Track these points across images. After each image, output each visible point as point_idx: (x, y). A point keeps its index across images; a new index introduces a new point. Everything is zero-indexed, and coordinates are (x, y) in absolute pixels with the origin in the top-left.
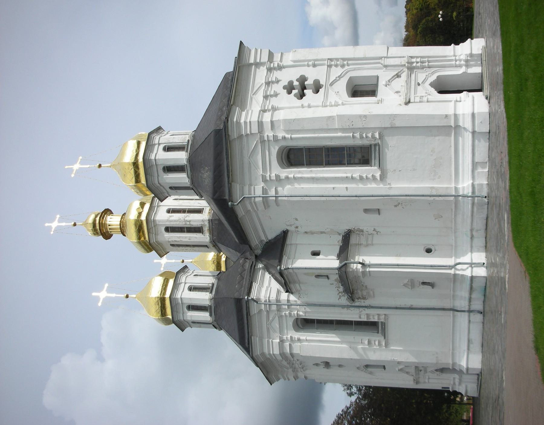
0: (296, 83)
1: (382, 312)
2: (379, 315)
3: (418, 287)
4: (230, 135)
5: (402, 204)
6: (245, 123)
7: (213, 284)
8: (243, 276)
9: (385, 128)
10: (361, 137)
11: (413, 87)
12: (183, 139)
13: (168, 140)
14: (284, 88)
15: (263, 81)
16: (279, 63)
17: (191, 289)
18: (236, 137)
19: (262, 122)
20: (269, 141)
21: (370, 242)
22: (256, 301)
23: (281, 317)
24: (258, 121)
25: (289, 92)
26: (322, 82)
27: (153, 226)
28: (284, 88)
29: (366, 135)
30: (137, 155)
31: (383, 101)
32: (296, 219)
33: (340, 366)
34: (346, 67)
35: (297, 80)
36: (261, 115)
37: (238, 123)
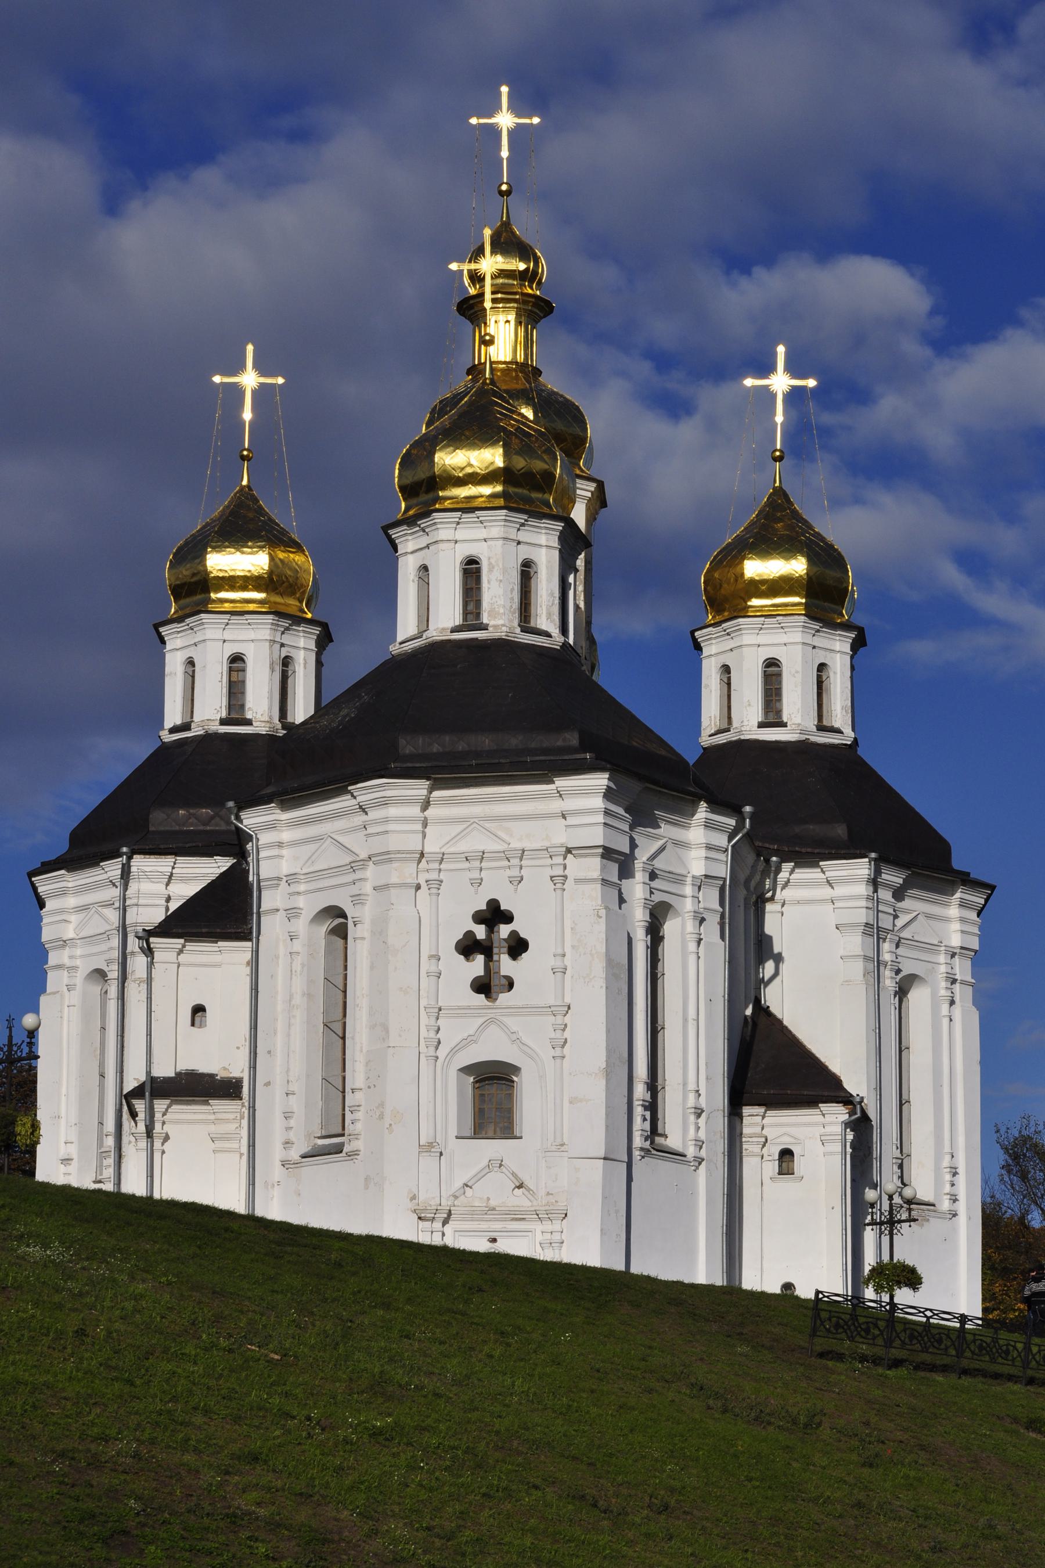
6: (386, 820)
7: (249, 722)
8: (213, 822)
11: (484, 1226)
12: (497, 609)
13: (493, 568)
15: (516, 844)
17: (237, 660)
19: (390, 861)
21: (219, 1144)
22: (126, 874)
24: (388, 853)
25: (479, 918)
26: (504, 998)
30: (461, 482)
31: (430, 1155)
34: (546, 1053)
35: (514, 934)
36: (408, 856)
37: (385, 803)
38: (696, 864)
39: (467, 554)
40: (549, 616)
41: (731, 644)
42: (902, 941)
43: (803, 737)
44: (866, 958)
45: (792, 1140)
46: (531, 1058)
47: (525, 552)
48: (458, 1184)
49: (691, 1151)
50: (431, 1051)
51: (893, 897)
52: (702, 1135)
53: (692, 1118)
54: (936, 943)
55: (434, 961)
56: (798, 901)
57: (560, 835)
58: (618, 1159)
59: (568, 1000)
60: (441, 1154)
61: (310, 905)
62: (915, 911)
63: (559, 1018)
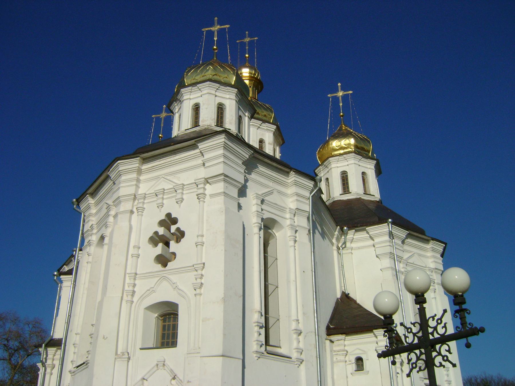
0: (173, 228)
14: (169, 215)
16: (208, 197)
19: (120, 202)
25: (162, 223)
28: (169, 215)
38: (291, 204)
39: (195, 102)
40: (231, 123)
41: (328, 170)
42: (408, 264)
43: (358, 197)
44: (392, 268)
45: (361, 352)
46: (183, 297)
47: (219, 100)
48: (139, 377)
49: (295, 355)
50: (129, 298)
51: (402, 243)
52: (301, 345)
53: (295, 336)
54: (424, 266)
55: (136, 249)
56: (359, 248)
57: (202, 173)
58: (234, 356)
59: (203, 261)
60: (129, 358)
62: (413, 252)
63: (200, 272)
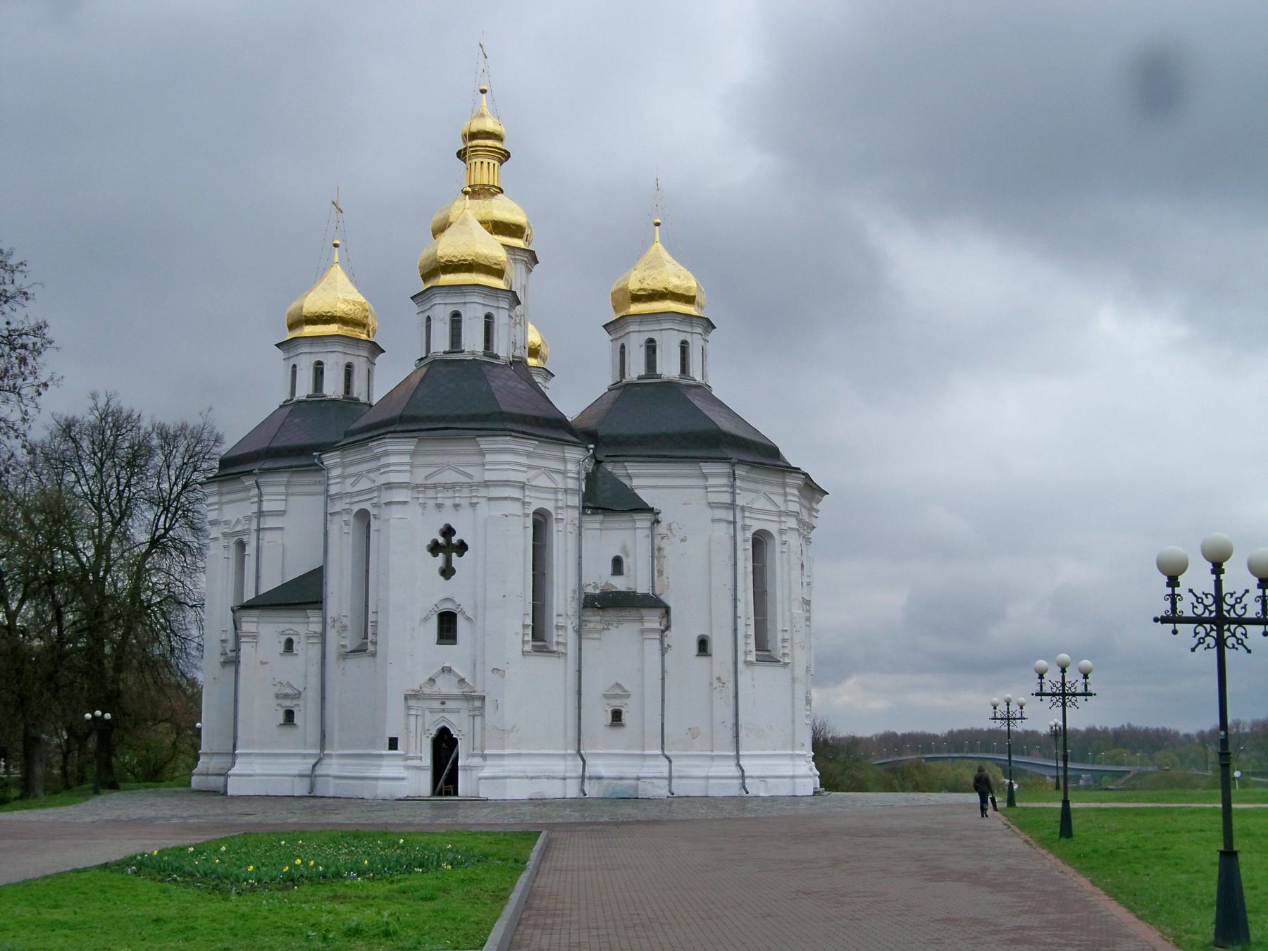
1: (571, 649)
2: (565, 644)
3: (608, 704)
4: (793, 474)
5: (723, 687)
9: (793, 670)
10: (784, 640)
18: (787, 480)
20: (780, 522)
23: (556, 491)
27: (517, 257)
29: (786, 647)
32: (683, 540)
33: (447, 572)
61: (757, 526)
